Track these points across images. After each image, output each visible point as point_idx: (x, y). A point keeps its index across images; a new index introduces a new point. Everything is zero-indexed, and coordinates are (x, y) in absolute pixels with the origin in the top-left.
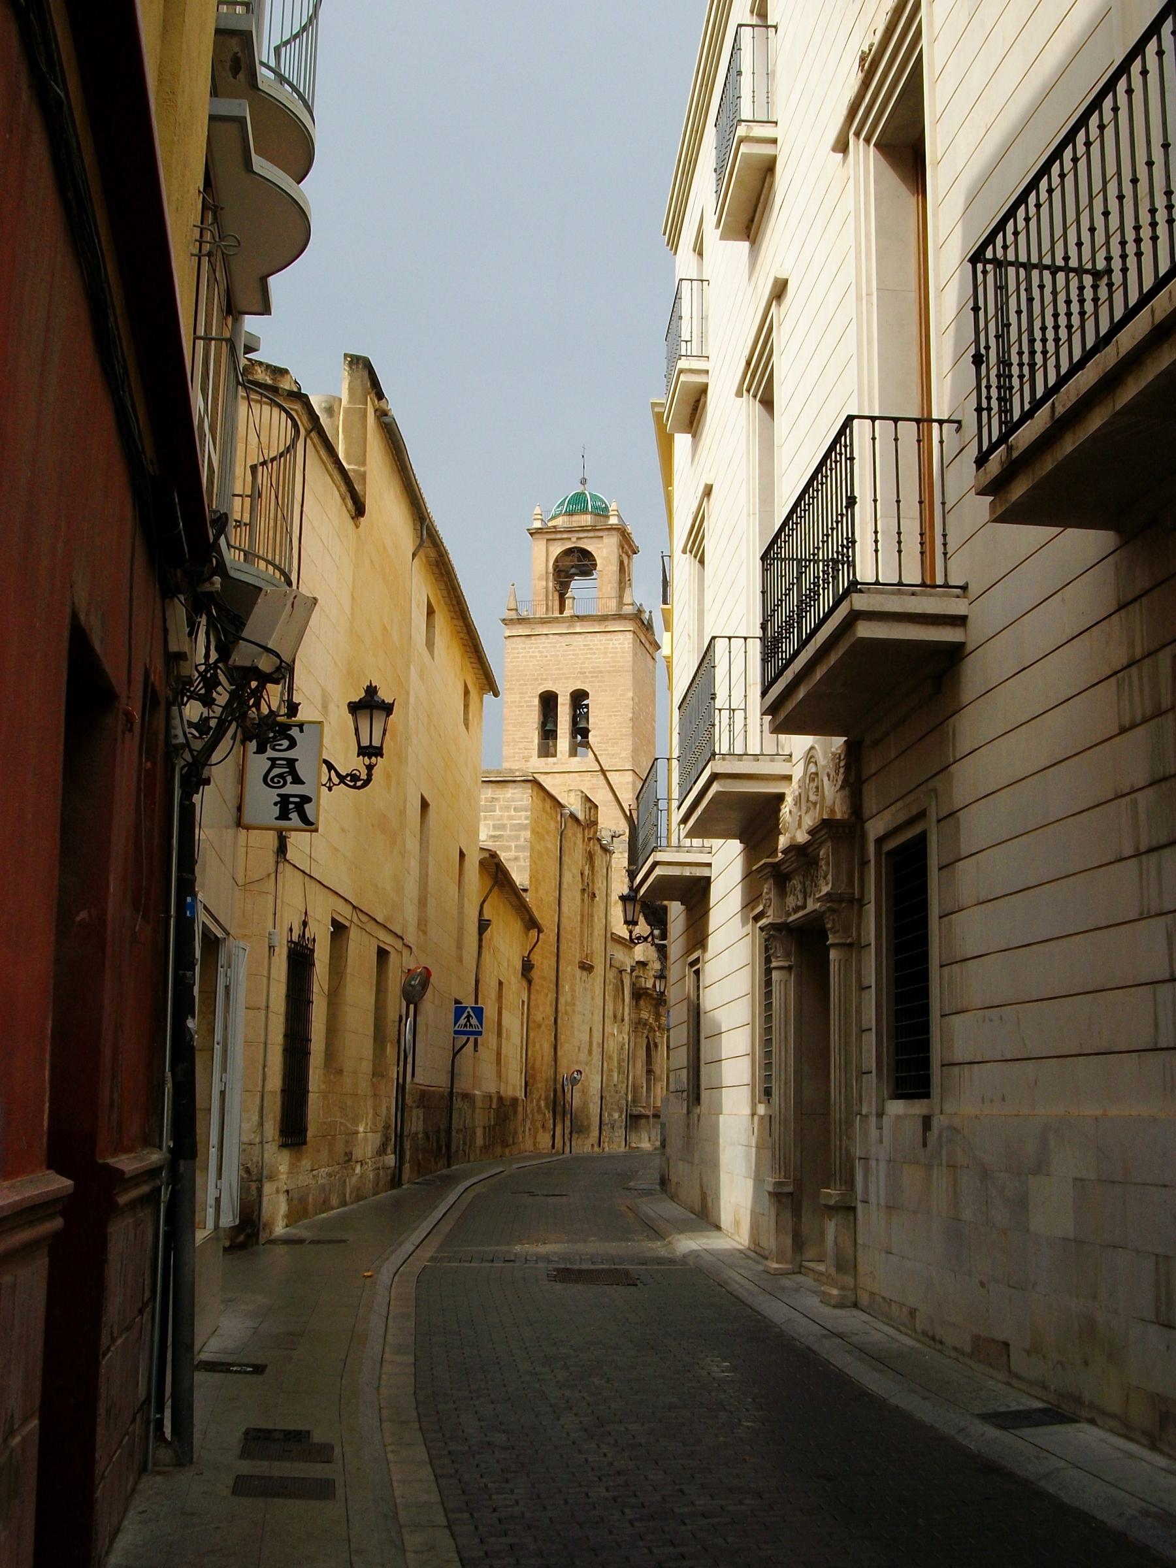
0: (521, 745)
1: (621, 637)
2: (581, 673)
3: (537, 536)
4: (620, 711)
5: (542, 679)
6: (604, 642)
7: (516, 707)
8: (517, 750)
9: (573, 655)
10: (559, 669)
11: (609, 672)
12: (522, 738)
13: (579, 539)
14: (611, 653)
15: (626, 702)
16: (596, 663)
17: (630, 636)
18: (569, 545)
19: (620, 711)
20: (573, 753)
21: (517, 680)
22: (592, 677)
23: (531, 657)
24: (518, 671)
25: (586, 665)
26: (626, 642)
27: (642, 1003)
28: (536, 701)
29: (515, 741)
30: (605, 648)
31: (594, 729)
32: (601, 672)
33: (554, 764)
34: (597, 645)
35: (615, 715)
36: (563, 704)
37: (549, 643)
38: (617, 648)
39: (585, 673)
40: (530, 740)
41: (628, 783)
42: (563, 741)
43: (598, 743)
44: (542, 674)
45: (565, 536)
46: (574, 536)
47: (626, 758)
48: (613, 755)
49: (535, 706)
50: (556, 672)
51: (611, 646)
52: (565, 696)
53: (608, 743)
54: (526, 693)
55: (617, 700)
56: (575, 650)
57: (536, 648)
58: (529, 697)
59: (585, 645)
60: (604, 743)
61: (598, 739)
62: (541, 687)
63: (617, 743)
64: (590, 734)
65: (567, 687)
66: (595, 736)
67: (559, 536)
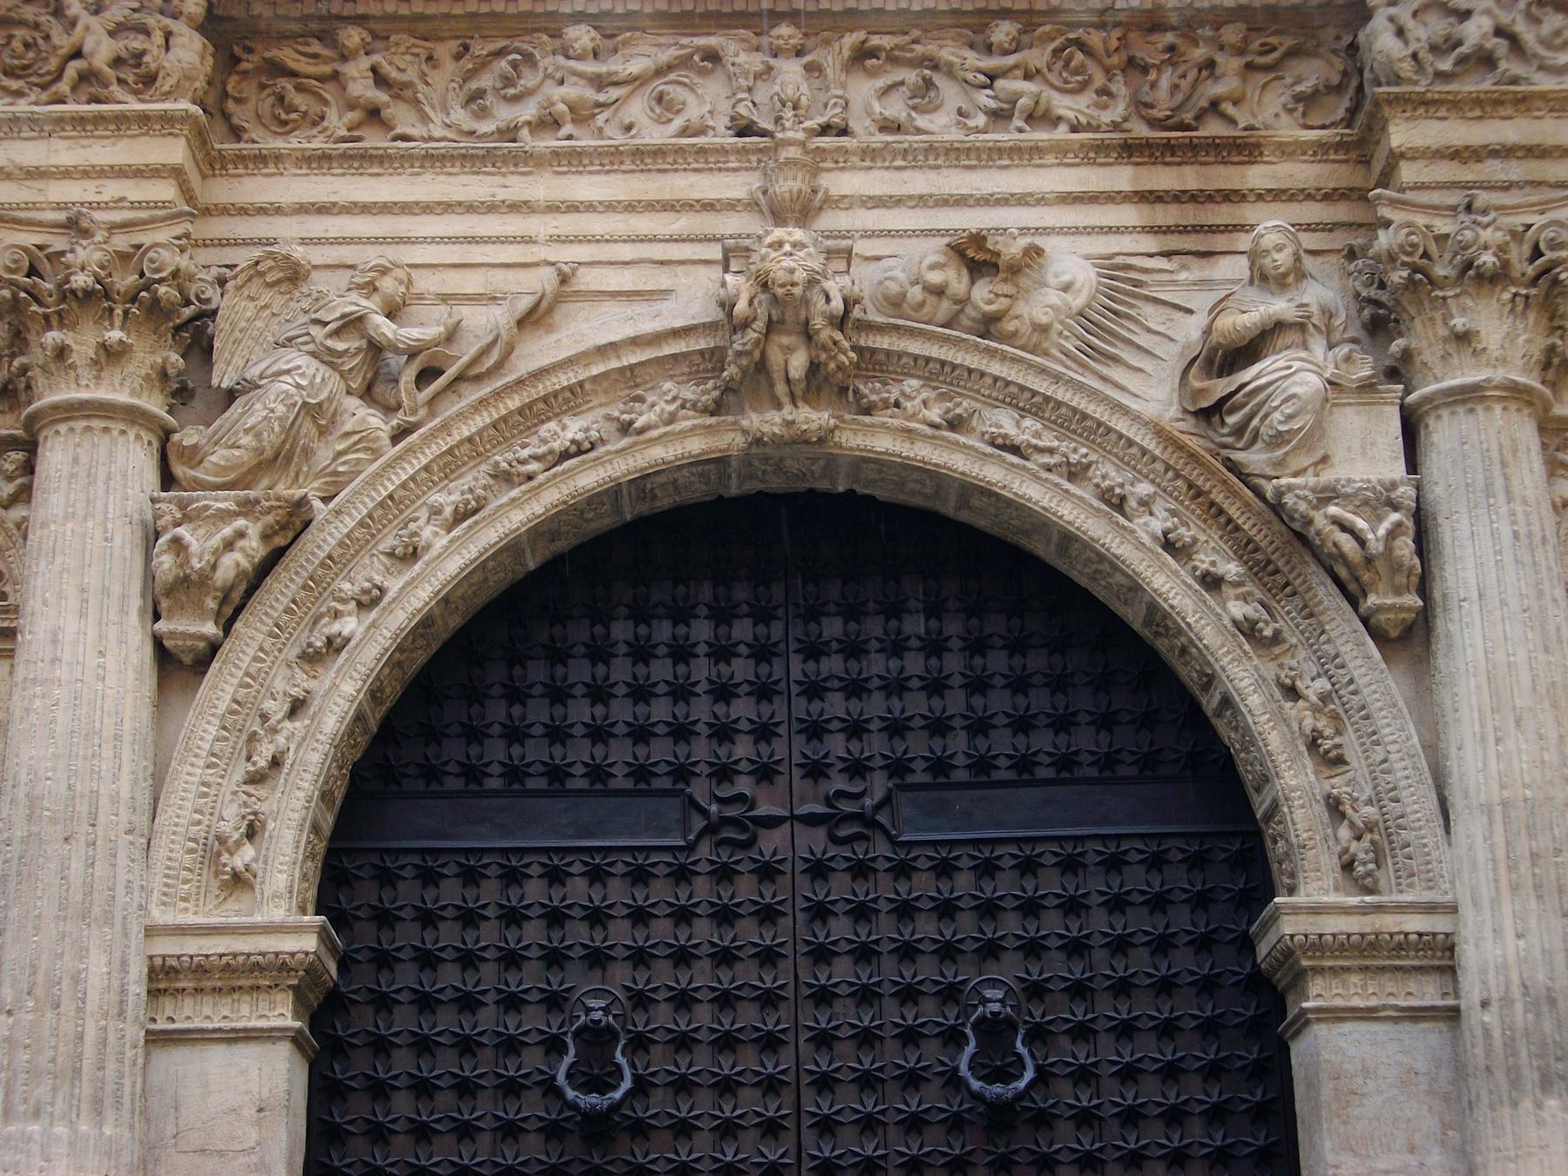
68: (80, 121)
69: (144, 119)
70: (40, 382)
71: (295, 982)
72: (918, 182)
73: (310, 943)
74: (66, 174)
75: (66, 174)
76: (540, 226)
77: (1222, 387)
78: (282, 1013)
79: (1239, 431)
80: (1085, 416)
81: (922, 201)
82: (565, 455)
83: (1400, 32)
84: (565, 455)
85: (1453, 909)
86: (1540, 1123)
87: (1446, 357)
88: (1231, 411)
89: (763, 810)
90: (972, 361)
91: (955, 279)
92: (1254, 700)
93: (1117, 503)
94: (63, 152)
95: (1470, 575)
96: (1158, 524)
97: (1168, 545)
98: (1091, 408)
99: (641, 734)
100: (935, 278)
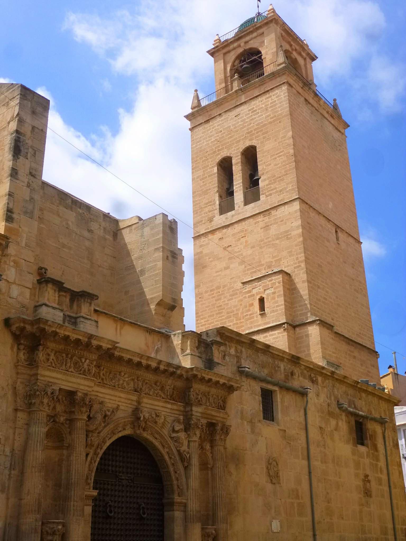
0: (207, 210)
1: (278, 91)
2: (248, 133)
3: (217, 54)
4: (283, 151)
5: (219, 150)
6: (264, 101)
7: (201, 180)
8: (203, 215)
9: (241, 121)
10: (231, 137)
11: (270, 123)
12: (207, 204)
13: (246, 42)
14: (271, 107)
15: (287, 141)
16: (259, 120)
17: (285, 88)
18: (240, 50)
19: (283, 151)
20: (246, 203)
21: (200, 158)
22: (257, 133)
23: (210, 137)
24: (200, 151)
25: (252, 125)
26: (282, 94)
27: (41, 355)
28: (215, 170)
29: (201, 208)
30: (266, 106)
31: (263, 174)
32: (265, 125)
33: (233, 216)
34: (259, 105)
35: (279, 157)
36: (237, 164)
37: (222, 120)
38: (275, 101)
39: (252, 131)
40: (212, 203)
41: (296, 212)
42: (239, 196)
43: (267, 185)
44: (219, 146)
45: (236, 45)
46: (242, 42)
47: (293, 189)
48: (281, 191)
49: (214, 174)
50: (229, 140)
51: (270, 101)
52: (237, 156)
53: (275, 182)
54: (208, 166)
55: (279, 143)
56: (241, 118)
57: (213, 128)
58: (210, 168)
59: (249, 110)
60: (272, 184)
61: (267, 182)
62: (219, 156)
63: (283, 180)
64: (260, 181)
65: (238, 149)
66: (265, 180)
67: (231, 47)
68: (85, 378)
69: (92, 380)
70: (76, 413)
71: (93, 498)
72: (150, 402)
73: (97, 494)
74: (82, 385)
75: (82, 385)
76: (117, 399)
77: (174, 435)
78: (90, 502)
79: (175, 441)
80: (162, 436)
81: (150, 404)
82: (119, 432)
83: (193, 395)
84: (119, 432)
85: (187, 499)
86: (196, 525)
87: (193, 436)
88: (176, 438)
89: (123, 478)
90: (154, 426)
91: (154, 416)
92: (172, 472)
93: (163, 446)
94: (82, 382)
95: (193, 462)
96: (167, 450)
97: (168, 453)
98: (163, 435)
99: (112, 466)
100: (153, 416)
